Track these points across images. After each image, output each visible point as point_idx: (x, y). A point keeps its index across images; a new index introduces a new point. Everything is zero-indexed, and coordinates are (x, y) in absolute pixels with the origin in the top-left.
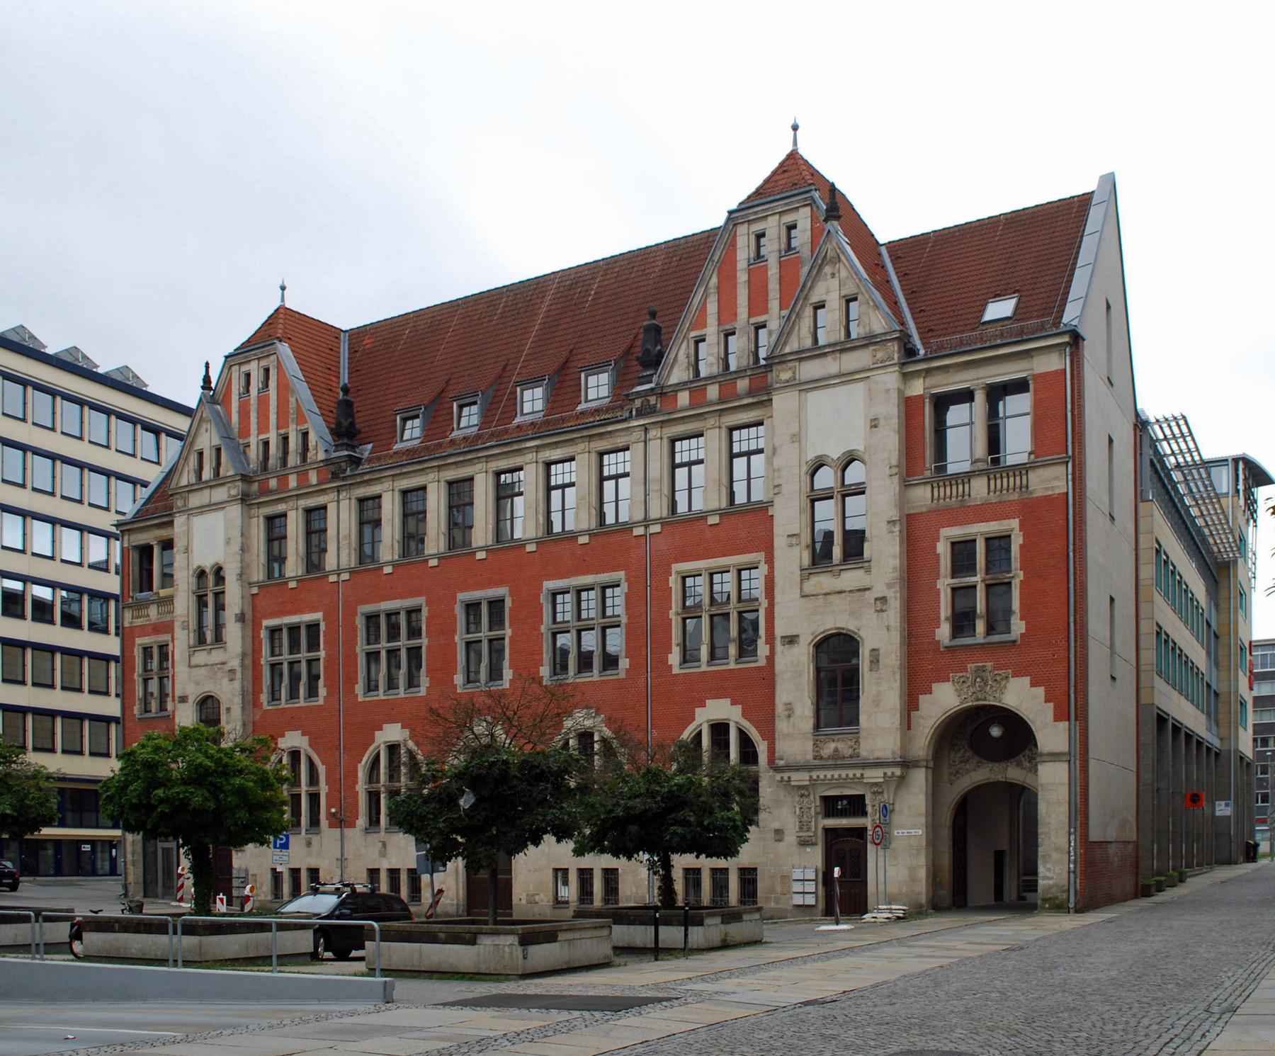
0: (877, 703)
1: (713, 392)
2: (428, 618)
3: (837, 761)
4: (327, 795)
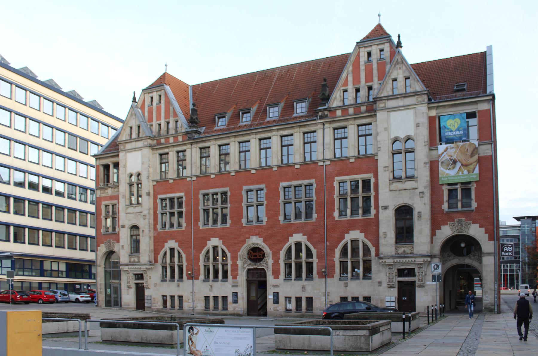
0: (420, 232)
1: (351, 111)
2: (230, 196)
3: (405, 255)
4: (186, 266)
